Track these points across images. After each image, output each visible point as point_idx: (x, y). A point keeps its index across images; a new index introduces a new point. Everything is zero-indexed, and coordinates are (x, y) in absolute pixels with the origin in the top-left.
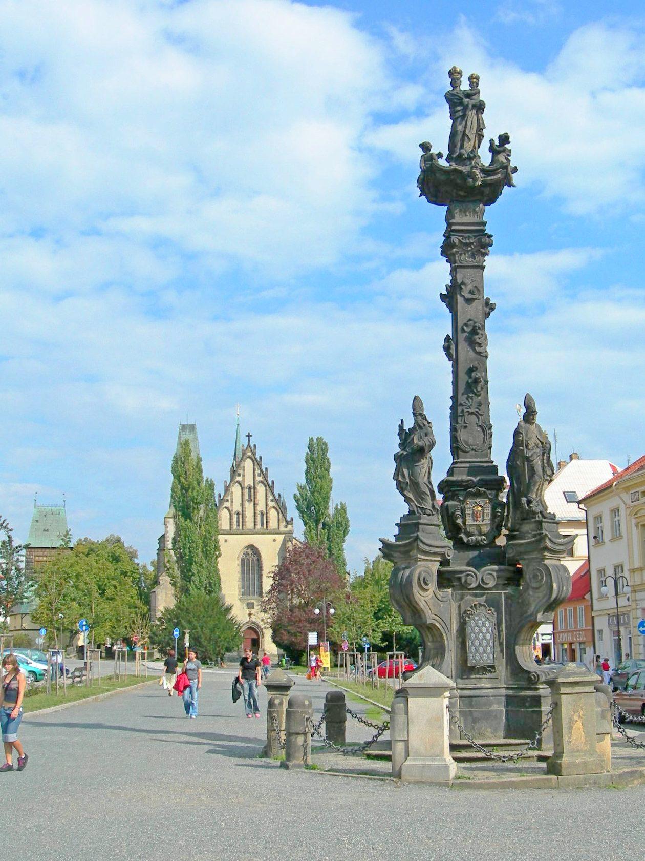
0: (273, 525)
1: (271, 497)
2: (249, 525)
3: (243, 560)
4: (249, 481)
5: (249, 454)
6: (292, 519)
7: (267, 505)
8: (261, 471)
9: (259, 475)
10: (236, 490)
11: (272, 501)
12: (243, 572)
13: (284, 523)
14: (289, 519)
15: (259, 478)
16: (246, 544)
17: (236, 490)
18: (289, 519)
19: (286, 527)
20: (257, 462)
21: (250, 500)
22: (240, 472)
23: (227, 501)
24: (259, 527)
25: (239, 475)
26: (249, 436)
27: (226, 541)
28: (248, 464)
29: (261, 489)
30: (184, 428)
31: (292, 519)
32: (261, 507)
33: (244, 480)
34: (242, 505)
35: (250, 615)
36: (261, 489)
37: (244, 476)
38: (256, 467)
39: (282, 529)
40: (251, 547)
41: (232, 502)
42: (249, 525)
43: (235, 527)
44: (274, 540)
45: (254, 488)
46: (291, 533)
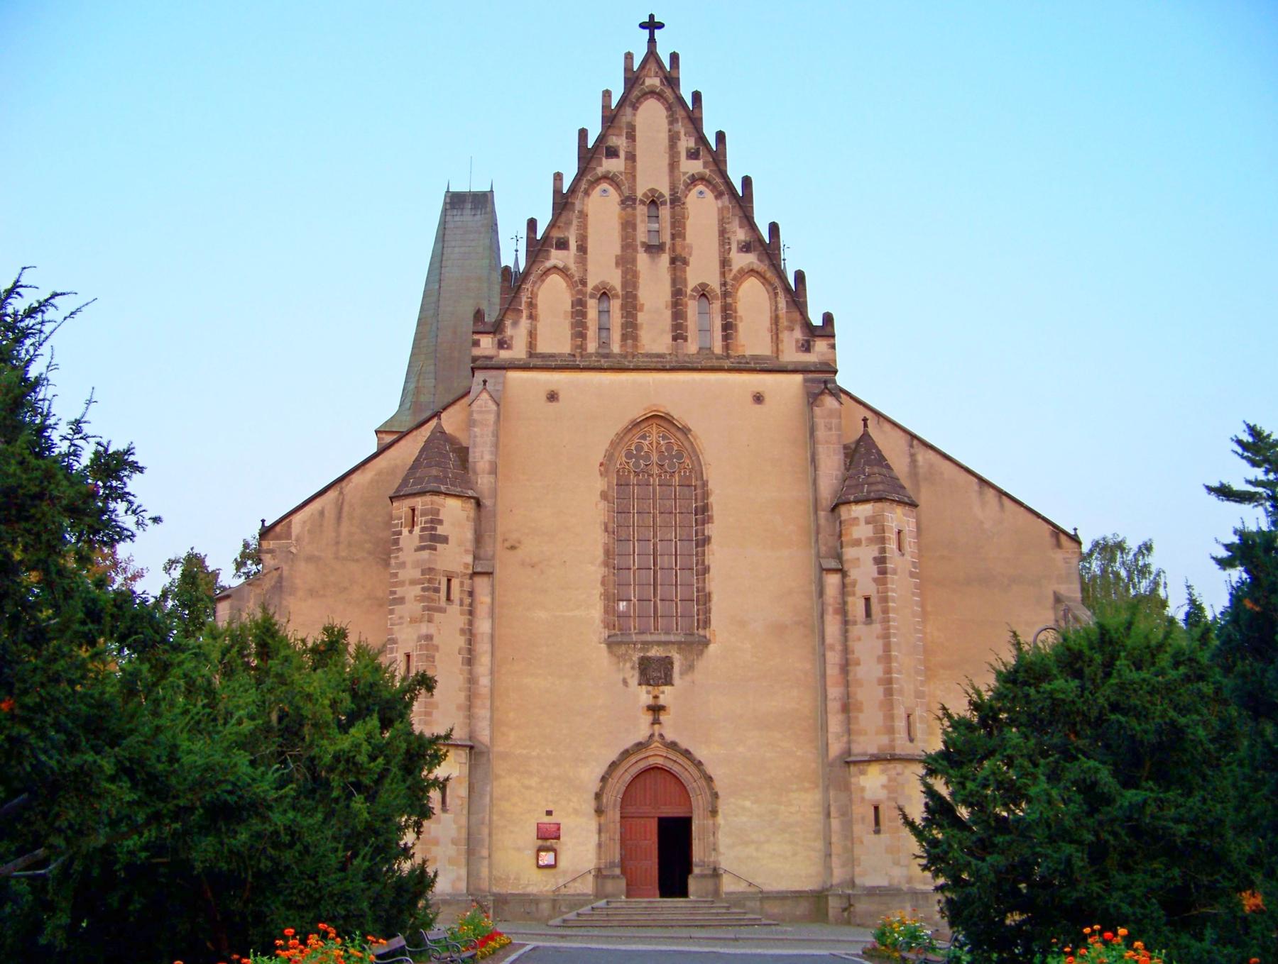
0: (754, 338)
1: (740, 235)
2: (655, 339)
3: (622, 484)
4: (652, 175)
5: (653, 81)
6: (828, 319)
7: (725, 263)
8: (702, 139)
9: (693, 155)
10: (602, 207)
11: (746, 248)
12: (617, 531)
13: (798, 334)
14: (817, 320)
15: (696, 167)
16: (638, 413)
17: (602, 207)
18: (817, 320)
19: (806, 347)
20: (689, 114)
21: (654, 249)
22: (620, 142)
23: (563, 245)
24: (692, 347)
25: (612, 153)
26: (652, 25)
27: (552, 397)
28: (651, 118)
29: (703, 210)
30: (455, 201)
31: (828, 319)
32: (703, 270)
33: (632, 174)
34: (626, 262)
35: (656, 710)
36: (703, 210)
37: (631, 157)
38: (680, 127)
39: (791, 355)
40: (659, 419)
41: (582, 249)
42: (655, 339)
43: (592, 347)
44: (758, 399)
45: (676, 201)
46: (830, 369)
